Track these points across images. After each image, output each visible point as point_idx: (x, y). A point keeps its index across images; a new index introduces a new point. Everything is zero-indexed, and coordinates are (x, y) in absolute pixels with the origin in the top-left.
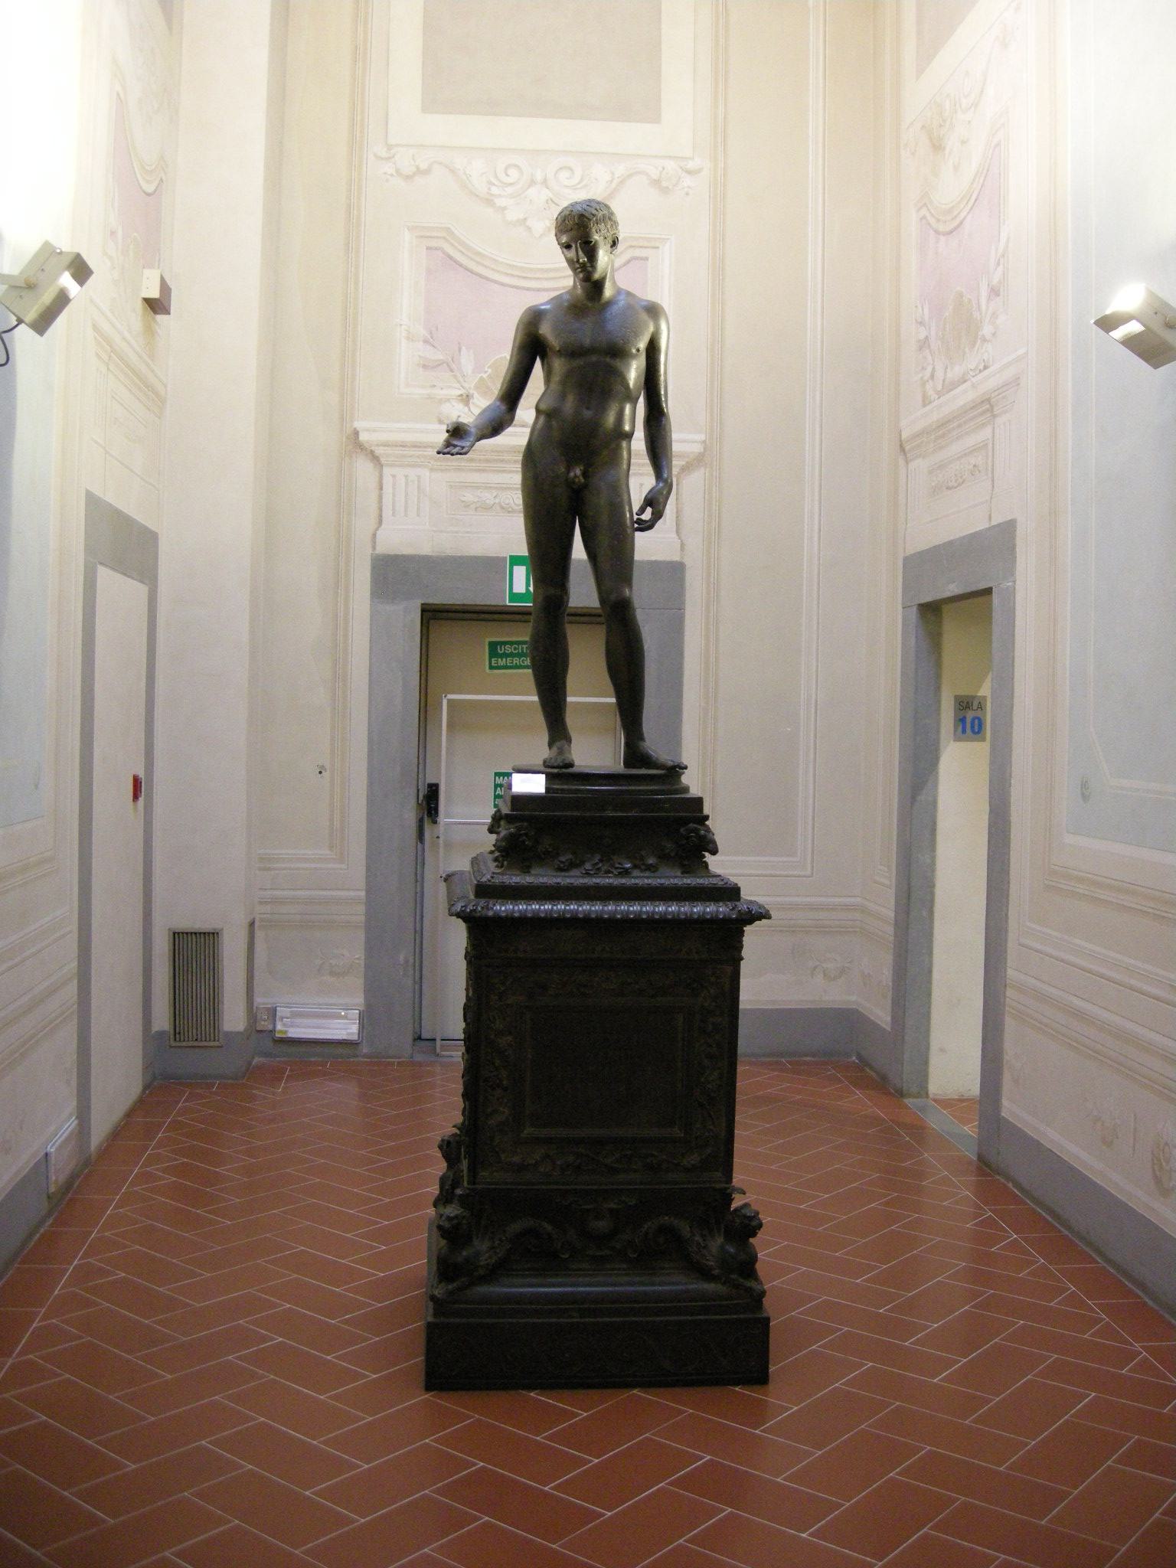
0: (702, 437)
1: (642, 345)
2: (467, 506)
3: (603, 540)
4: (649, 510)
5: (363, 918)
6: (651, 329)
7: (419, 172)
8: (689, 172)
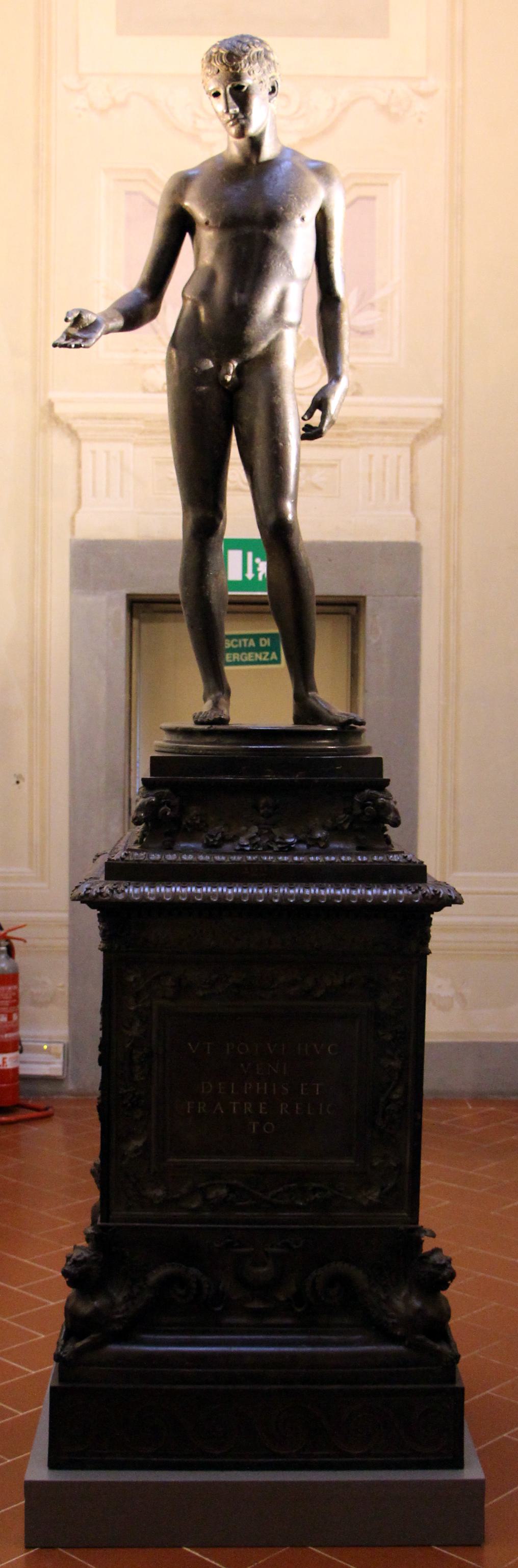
0: (439, 401)
1: (310, 213)
3: (260, 449)
4: (318, 413)
5: (65, 942)
8: (424, 95)
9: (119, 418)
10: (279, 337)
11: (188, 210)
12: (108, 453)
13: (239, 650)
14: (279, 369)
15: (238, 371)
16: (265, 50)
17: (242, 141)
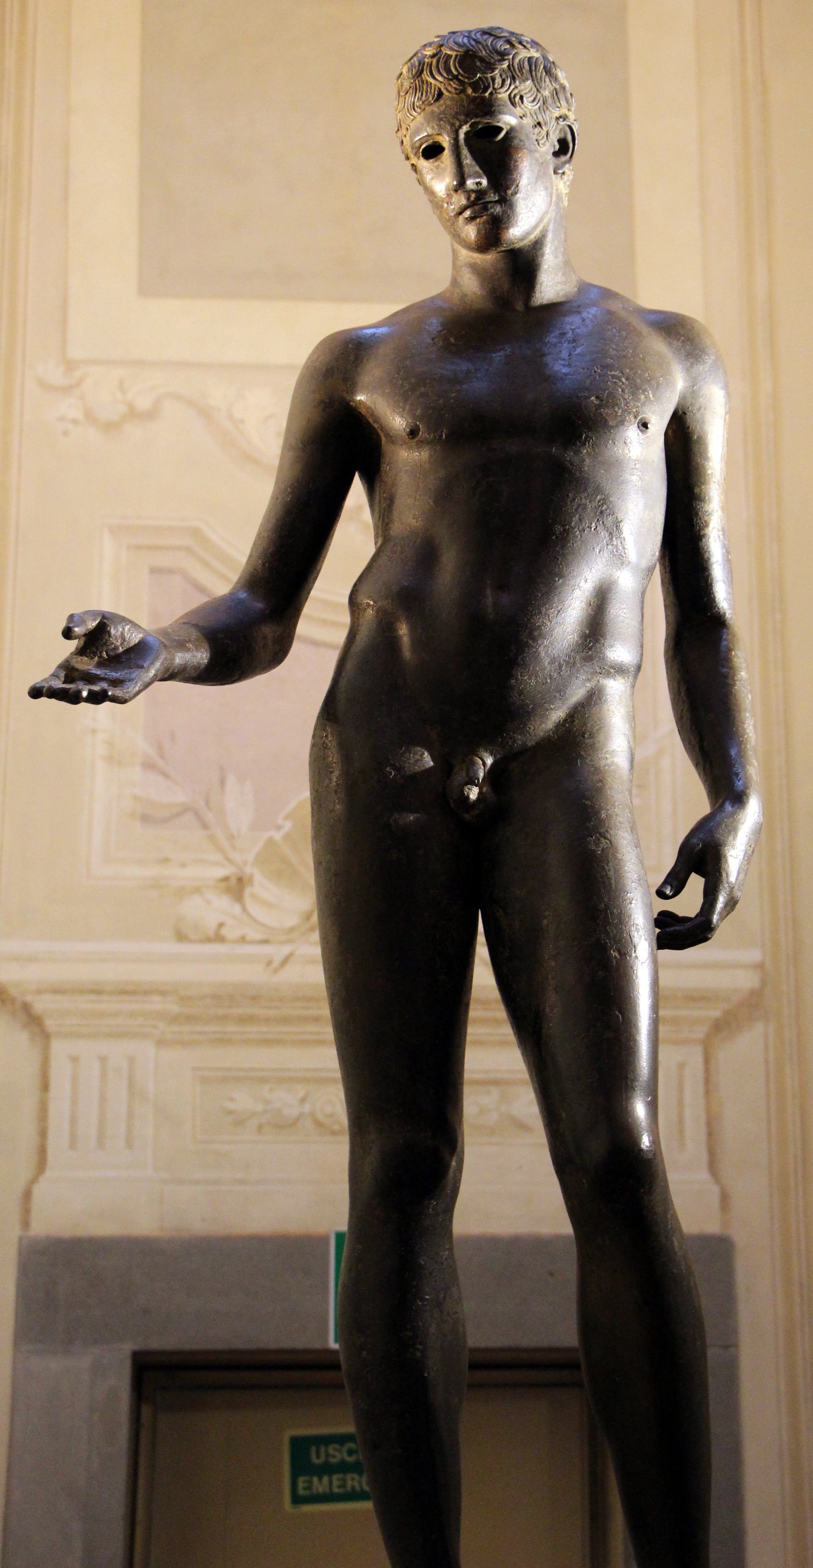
2: (239, 1121)
4: (696, 883)
6: (679, 382)
7: (133, 414)
9: (126, 991)
10: (594, 697)
11: (363, 411)
12: (103, 1060)
14: (597, 770)
15: (493, 774)
16: (545, 58)
17: (489, 258)
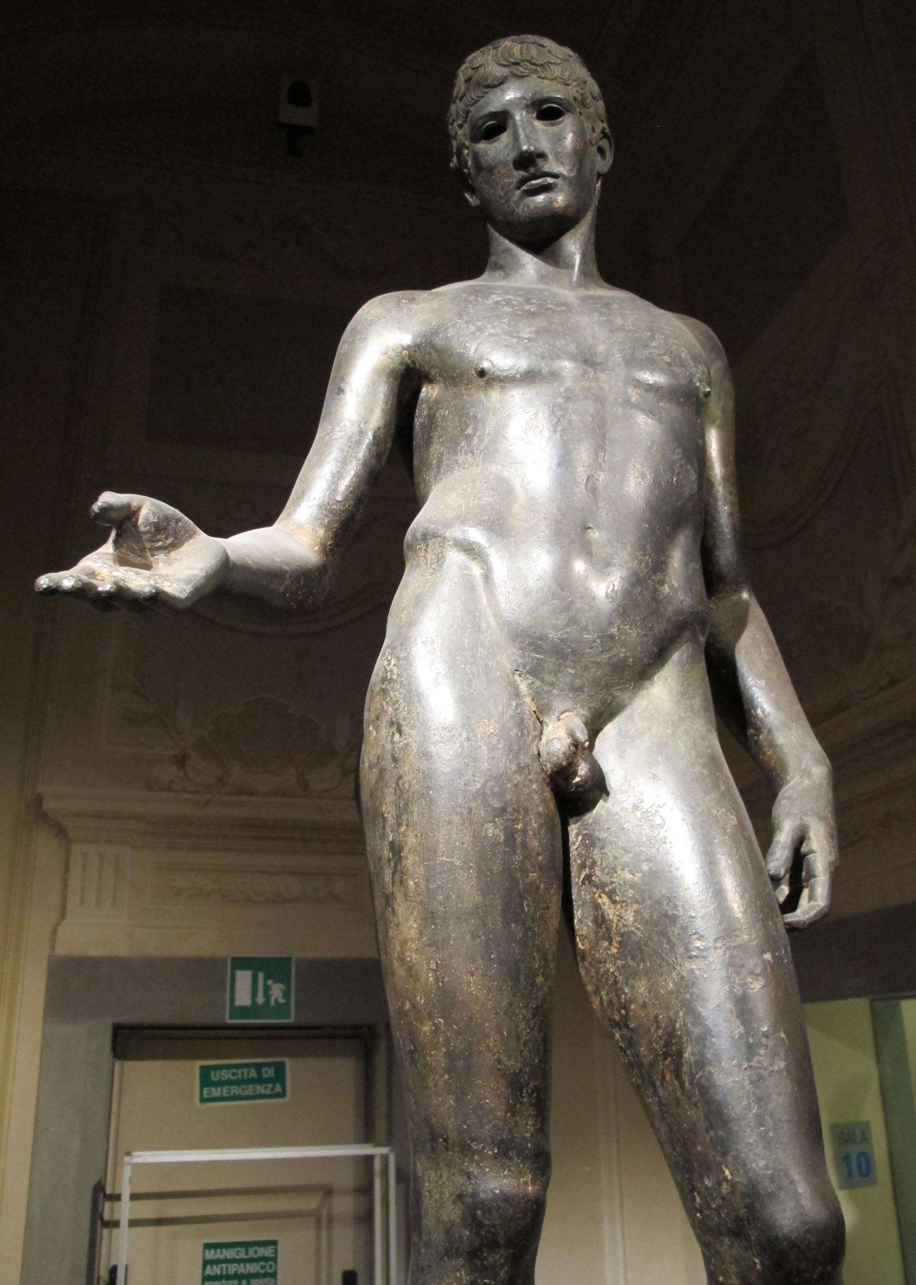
13: (238, 1083)
